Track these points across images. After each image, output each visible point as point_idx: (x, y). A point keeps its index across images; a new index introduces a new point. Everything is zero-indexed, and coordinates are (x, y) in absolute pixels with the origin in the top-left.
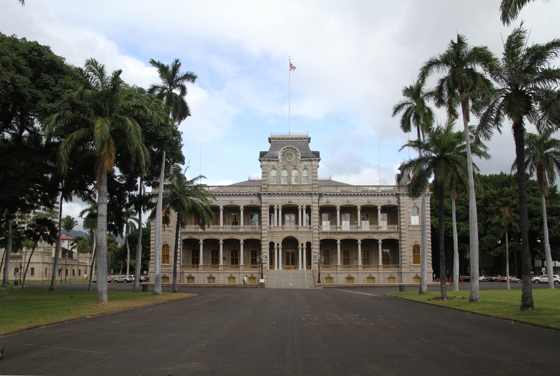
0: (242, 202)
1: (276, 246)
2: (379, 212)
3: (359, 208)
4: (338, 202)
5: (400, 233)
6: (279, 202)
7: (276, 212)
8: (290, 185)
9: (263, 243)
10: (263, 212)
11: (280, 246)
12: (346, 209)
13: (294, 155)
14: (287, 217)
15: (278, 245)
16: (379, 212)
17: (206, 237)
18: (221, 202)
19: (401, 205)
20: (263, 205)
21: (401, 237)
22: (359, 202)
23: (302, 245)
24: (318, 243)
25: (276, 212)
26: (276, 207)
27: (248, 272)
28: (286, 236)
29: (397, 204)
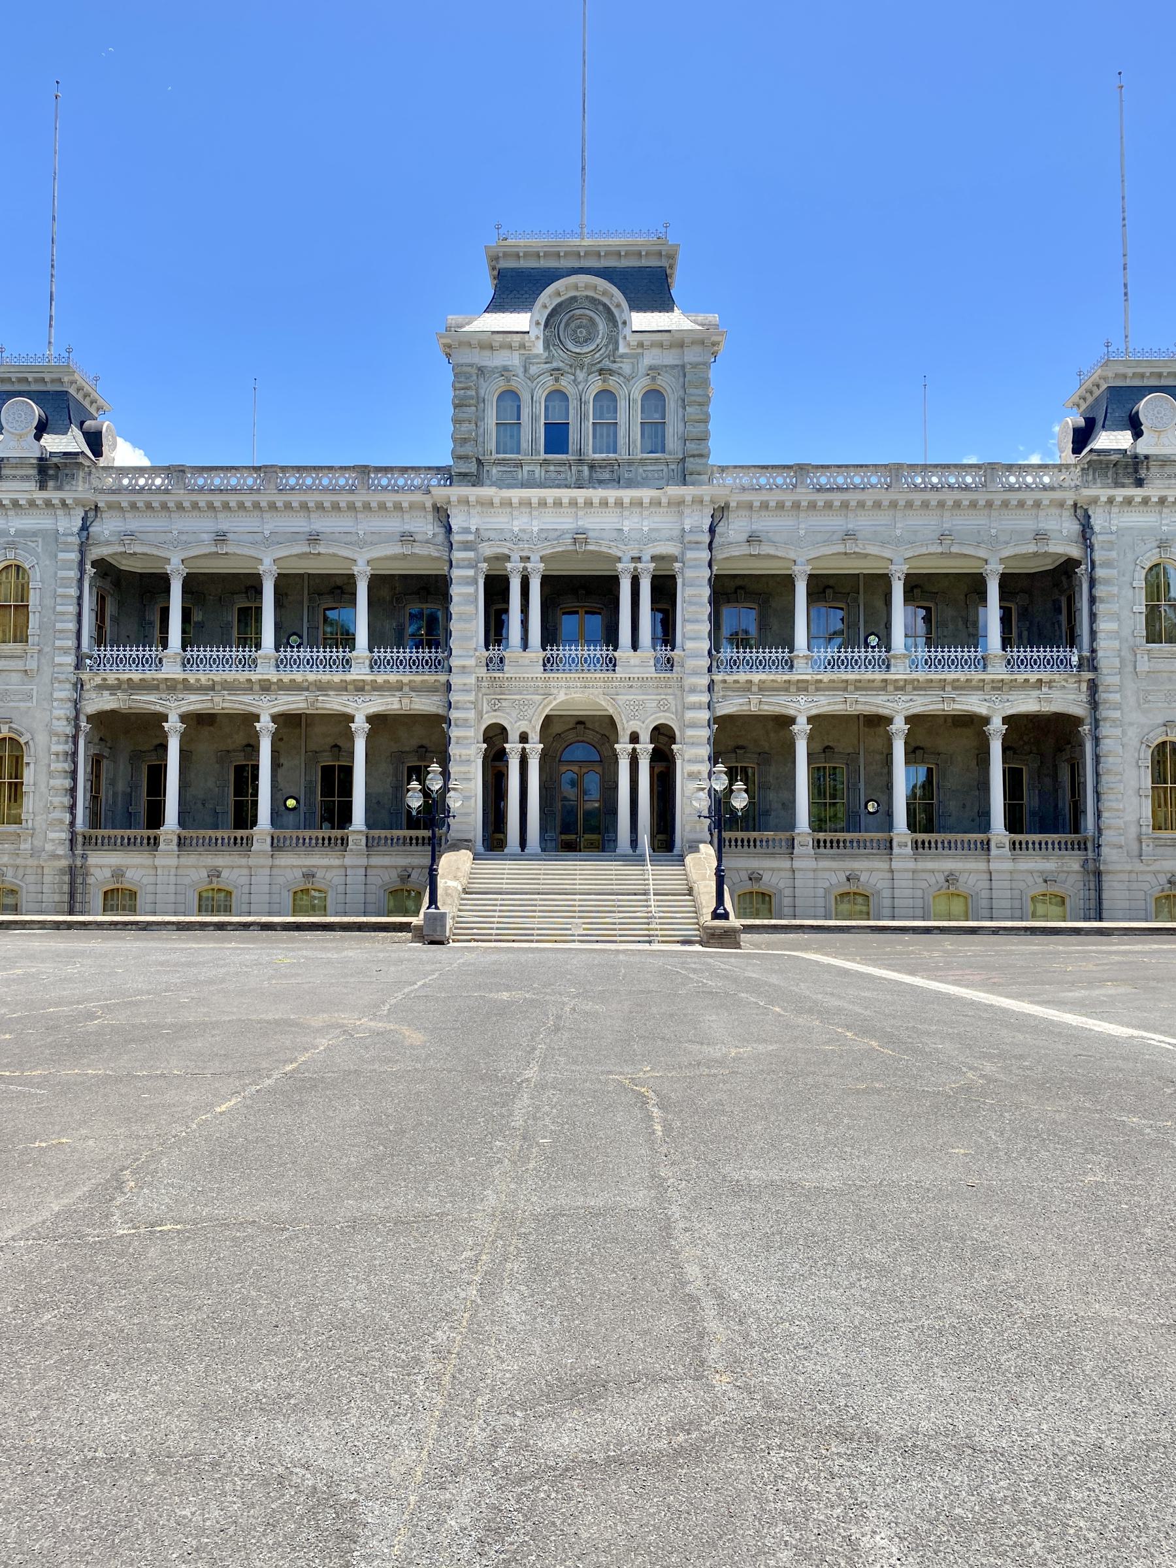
5: (1093, 687)
8: (580, 462)
9: (454, 733)
13: (602, 326)
14: (568, 624)
15: (524, 738)
17: (195, 703)
19: (1098, 556)
20: (457, 555)
21: (1094, 704)
23: (634, 738)
24: (705, 733)
26: (514, 569)
27: (386, 861)
28: (562, 697)
29: (1075, 552)
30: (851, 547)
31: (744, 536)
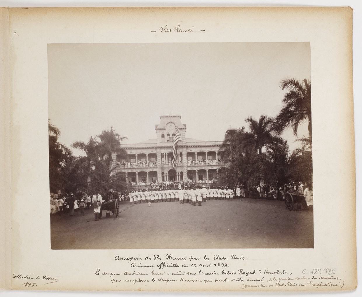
0: (147, 152)
1: (165, 174)
2: (217, 155)
3: (206, 153)
4: (196, 150)
6: (166, 151)
7: (164, 156)
10: (158, 157)
11: (167, 175)
12: (200, 154)
15: (166, 174)
16: (217, 155)
18: (136, 152)
22: (206, 150)
23: (178, 173)
25: (164, 156)
30: (201, 151)
31: (189, 150)
